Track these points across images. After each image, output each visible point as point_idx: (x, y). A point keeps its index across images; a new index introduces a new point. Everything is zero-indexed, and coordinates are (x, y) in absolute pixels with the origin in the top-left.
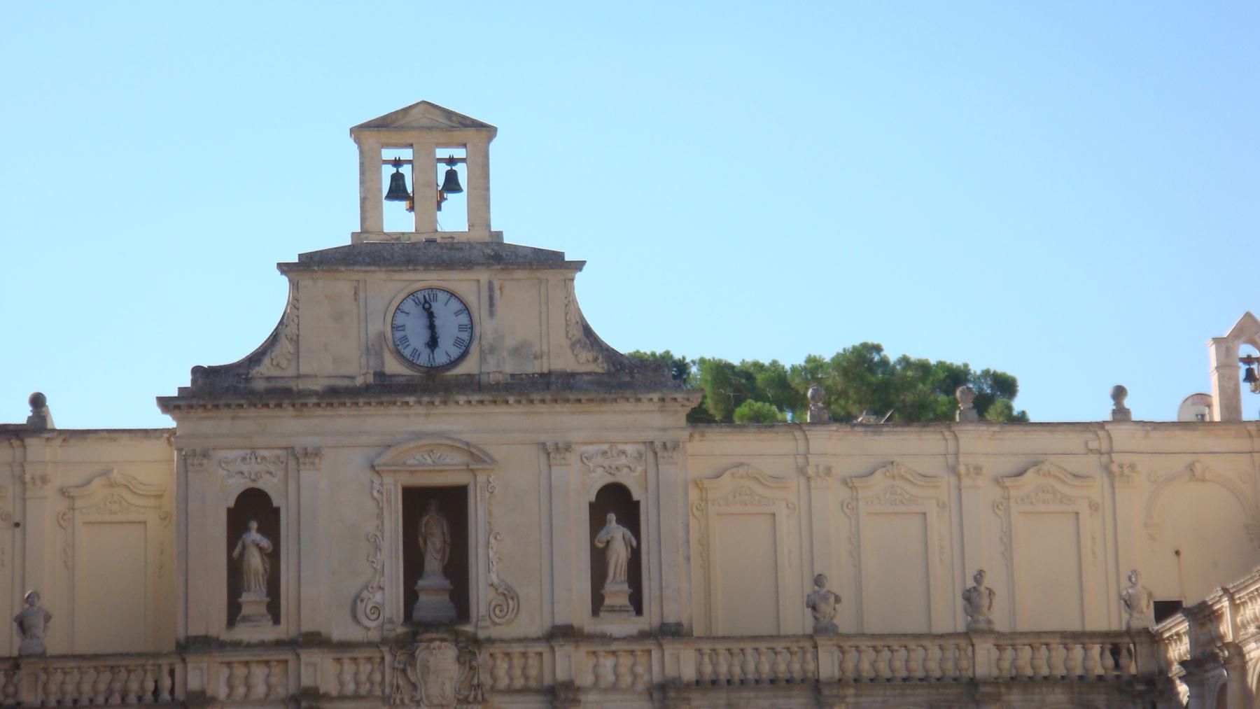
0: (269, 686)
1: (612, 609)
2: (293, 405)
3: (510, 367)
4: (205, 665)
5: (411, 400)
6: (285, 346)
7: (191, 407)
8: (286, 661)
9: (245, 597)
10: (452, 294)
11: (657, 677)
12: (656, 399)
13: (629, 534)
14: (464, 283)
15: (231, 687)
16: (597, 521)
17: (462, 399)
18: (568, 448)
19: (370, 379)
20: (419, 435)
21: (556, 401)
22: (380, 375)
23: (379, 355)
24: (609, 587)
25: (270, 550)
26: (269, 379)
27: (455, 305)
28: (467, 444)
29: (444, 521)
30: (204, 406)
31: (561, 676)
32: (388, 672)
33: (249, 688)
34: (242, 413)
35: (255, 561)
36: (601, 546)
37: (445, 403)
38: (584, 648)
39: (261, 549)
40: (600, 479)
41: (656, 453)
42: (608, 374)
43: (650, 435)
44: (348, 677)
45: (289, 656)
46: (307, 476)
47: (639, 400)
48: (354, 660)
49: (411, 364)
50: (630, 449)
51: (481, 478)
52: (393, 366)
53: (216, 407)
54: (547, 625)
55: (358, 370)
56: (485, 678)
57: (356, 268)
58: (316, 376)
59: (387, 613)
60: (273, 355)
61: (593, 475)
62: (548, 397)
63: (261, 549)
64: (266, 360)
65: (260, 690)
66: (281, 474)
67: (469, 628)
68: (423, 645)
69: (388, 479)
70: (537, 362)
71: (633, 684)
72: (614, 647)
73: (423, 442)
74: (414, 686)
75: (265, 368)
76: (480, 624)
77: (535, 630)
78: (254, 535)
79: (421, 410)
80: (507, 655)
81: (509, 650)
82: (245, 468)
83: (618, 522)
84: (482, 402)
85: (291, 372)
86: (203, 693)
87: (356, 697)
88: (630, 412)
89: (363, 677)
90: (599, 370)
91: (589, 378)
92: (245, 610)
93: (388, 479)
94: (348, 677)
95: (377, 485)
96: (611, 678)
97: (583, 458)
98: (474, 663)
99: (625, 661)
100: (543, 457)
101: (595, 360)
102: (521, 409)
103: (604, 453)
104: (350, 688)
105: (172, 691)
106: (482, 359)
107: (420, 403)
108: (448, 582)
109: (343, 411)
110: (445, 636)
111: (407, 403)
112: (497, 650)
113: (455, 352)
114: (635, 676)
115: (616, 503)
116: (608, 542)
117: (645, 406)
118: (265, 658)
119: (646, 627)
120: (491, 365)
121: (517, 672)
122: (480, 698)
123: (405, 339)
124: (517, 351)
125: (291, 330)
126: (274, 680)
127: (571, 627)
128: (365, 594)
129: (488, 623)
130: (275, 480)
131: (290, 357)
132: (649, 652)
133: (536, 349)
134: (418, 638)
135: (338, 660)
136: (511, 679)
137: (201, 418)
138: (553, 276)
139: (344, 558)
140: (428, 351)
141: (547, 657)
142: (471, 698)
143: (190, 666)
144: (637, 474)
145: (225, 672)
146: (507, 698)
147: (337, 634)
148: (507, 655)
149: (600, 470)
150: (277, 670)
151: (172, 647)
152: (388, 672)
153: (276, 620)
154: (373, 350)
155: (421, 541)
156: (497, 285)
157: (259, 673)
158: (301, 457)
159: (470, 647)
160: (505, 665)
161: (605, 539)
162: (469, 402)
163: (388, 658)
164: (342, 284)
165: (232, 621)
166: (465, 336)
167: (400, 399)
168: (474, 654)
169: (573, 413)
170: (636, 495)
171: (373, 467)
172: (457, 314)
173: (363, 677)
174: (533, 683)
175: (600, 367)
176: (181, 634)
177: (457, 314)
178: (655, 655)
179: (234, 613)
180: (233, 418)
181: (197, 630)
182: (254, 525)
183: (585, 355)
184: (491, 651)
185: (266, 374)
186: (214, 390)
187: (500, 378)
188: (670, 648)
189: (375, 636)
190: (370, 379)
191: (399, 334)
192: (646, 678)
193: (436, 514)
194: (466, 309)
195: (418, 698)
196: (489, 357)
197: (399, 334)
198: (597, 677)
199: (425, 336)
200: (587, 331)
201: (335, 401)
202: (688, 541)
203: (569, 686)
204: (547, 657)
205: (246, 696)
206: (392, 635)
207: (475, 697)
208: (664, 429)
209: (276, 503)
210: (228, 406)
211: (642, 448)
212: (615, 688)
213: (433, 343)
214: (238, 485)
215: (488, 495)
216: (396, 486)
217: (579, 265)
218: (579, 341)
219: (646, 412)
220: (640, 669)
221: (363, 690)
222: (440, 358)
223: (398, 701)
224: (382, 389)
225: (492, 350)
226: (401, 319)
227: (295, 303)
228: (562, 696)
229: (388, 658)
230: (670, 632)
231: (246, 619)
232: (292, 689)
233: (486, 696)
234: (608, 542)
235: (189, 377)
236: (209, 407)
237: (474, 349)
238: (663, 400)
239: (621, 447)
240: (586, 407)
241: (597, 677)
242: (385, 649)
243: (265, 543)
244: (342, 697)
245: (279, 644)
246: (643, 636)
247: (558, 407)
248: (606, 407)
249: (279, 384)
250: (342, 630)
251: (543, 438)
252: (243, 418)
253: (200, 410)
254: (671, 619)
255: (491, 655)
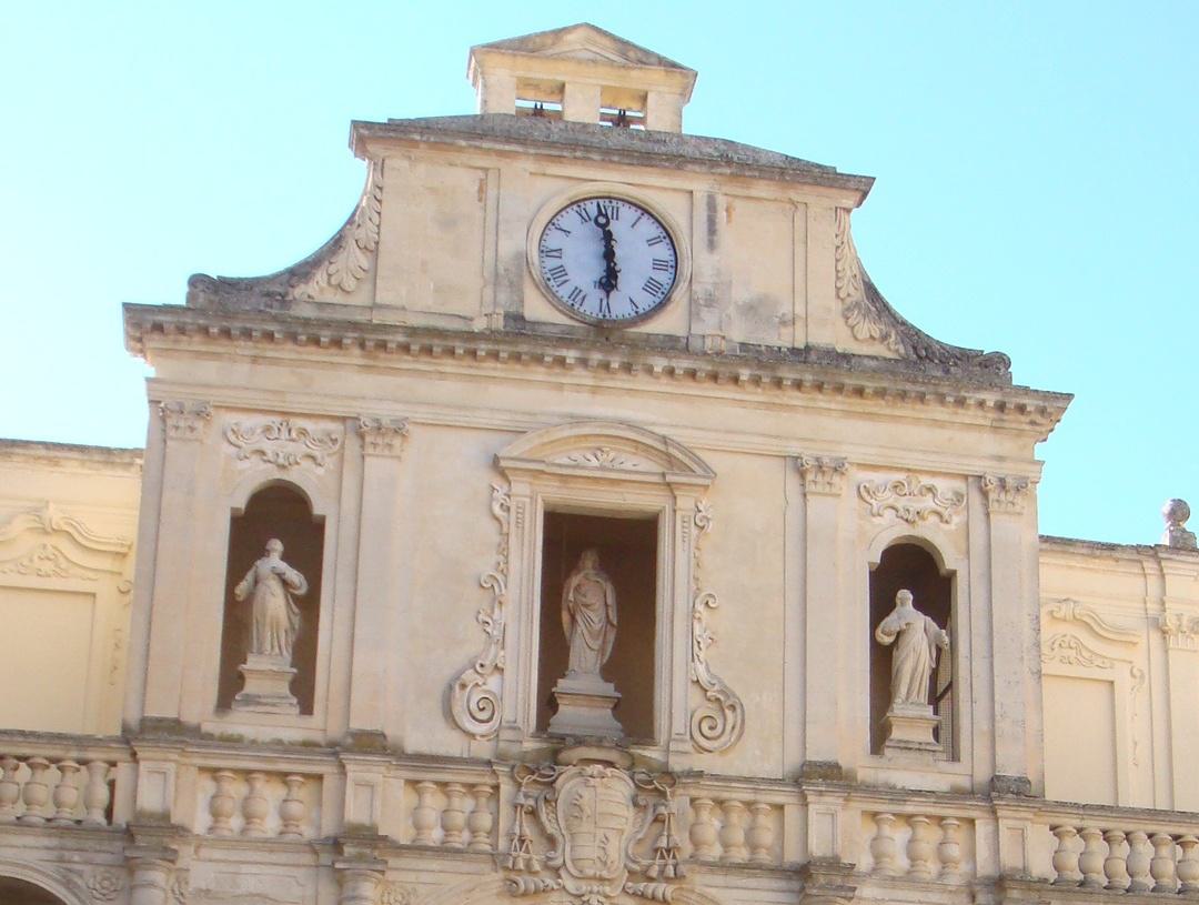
0: (286, 819)
1: (906, 747)
2: (362, 346)
3: (738, 333)
4: (171, 767)
5: (571, 355)
6: (353, 258)
7: (181, 330)
8: (319, 778)
9: (252, 663)
10: (645, 211)
11: (985, 867)
12: (991, 404)
13: (934, 626)
14: (664, 192)
15: (216, 814)
16: (881, 606)
17: (659, 364)
18: (838, 469)
19: (499, 323)
20: (578, 420)
21: (819, 387)
22: (516, 318)
23: (516, 288)
24: (899, 708)
25: (302, 591)
26: (321, 305)
27: (648, 229)
28: (665, 440)
29: (609, 589)
30: (205, 331)
31: (818, 848)
32: (505, 810)
33: (249, 817)
34: (270, 351)
35: (274, 606)
36: (887, 640)
37: (627, 368)
38: (860, 805)
39: (285, 584)
40: (890, 531)
41: (985, 494)
42: (904, 360)
43: (976, 467)
44: (431, 815)
45: (327, 769)
46: (376, 467)
47: (961, 402)
48: (443, 785)
49: (570, 311)
50: (942, 485)
51: (685, 502)
52: (537, 309)
53: (226, 333)
54: (793, 760)
55: (474, 305)
56: (680, 838)
57: (486, 145)
58: (404, 308)
59: (507, 713)
60: (332, 269)
61: (877, 520)
62: (808, 377)
63: (285, 584)
64: (320, 276)
65: (270, 825)
66: (330, 463)
67: (653, 754)
68: (572, 770)
69: (521, 488)
70: (786, 331)
71: (941, 875)
72: (909, 809)
73: (586, 430)
74: (551, 841)
75: (317, 287)
76: (673, 747)
77: (771, 767)
78: (274, 558)
79: (584, 377)
80: (720, 803)
81: (725, 795)
82: (269, 447)
83: (918, 605)
84: (692, 374)
85: (361, 298)
86: (166, 816)
87: (444, 851)
88: (936, 423)
89: (459, 819)
90: (890, 355)
91: (873, 363)
92: (251, 687)
93: (521, 488)
94: (431, 815)
95: (499, 495)
96: (900, 863)
97: (863, 493)
98: (662, 809)
99: (929, 836)
100: (793, 481)
101: (885, 338)
102: (759, 395)
103: (897, 486)
104: (435, 836)
105: (109, 813)
106: (693, 313)
107: (584, 362)
108: (609, 689)
109: (449, 366)
110: (613, 756)
111: (561, 362)
112: (705, 794)
113: (646, 301)
114: (945, 861)
115: (911, 574)
116: (899, 634)
117: (970, 415)
118: (284, 767)
119: (964, 782)
120: (708, 324)
121: (738, 836)
122: (670, 872)
123: (560, 272)
124: (751, 309)
125: (366, 233)
126: (295, 808)
127: (837, 766)
128: (469, 676)
129: (688, 747)
130: (320, 471)
131: (361, 274)
132: (972, 822)
133: (785, 309)
134: (563, 756)
135: (413, 783)
136: (726, 846)
137: (199, 355)
138: (818, 201)
139: (434, 595)
140: (602, 294)
141: (792, 813)
142: (654, 873)
143: (143, 766)
144: (952, 527)
145: (207, 786)
146: (719, 879)
147: (414, 742)
148: (720, 803)
149: (889, 514)
150: (302, 792)
151: (118, 732)
152: (505, 810)
153: (307, 708)
154: (508, 277)
155: (565, 617)
156: (721, 201)
157: (269, 796)
158: (364, 433)
159: (655, 785)
160: (717, 824)
161: (895, 628)
162: (671, 372)
163: (506, 788)
164: (457, 176)
165: (225, 702)
166: (664, 278)
167: (550, 353)
168: (662, 794)
169: (848, 414)
170: (950, 560)
171: (495, 464)
172: (651, 242)
173: (459, 819)
174: (764, 857)
175: (890, 350)
176: (133, 717)
177: (651, 242)
178: (983, 828)
179: (231, 685)
180: (255, 360)
181: (161, 708)
182: (277, 546)
183: (867, 328)
184: (694, 793)
185: (319, 298)
186: (225, 314)
187: (724, 346)
188: (1009, 819)
189: (483, 750)
190: (499, 323)
191: (552, 263)
192: (964, 867)
193: (603, 558)
194: (669, 236)
195: (559, 862)
196: (705, 313)
197: (552, 263)
198: (878, 857)
199: (597, 270)
200: (871, 292)
201: (438, 345)
202: (1038, 645)
203: (834, 864)
204: (792, 813)
205: (244, 831)
206: (515, 749)
207: (662, 872)
208: (1001, 459)
209: (318, 509)
210: (247, 334)
211: (960, 485)
212: (910, 878)
213: (609, 281)
214: (253, 475)
215: (694, 531)
216: (533, 499)
217: (861, 187)
218: (857, 305)
219: (970, 426)
220: (955, 851)
221: (460, 839)
222: (620, 306)
223: (521, 865)
224: (516, 339)
225: (710, 302)
226: (555, 239)
227: (377, 192)
228: (822, 880)
229: (506, 788)
230: (1003, 792)
231: (251, 700)
232: (329, 828)
233: (683, 868)
234: (899, 634)
235: (185, 289)
236: (214, 330)
237: (680, 295)
238: (1001, 407)
239: (926, 480)
240: (870, 405)
241: (878, 857)
242: (502, 769)
243: (294, 576)
244: (418, 849)
245: (308, 745)
246: (957, 795)
247: (822, 401)
248: (906, 410)
249: (339, 315)
250: (424, 734)
251: (794, 448)
252: (275, 361)
253: (197, 338)
254: (1010, 770)
255: (693, 800)
